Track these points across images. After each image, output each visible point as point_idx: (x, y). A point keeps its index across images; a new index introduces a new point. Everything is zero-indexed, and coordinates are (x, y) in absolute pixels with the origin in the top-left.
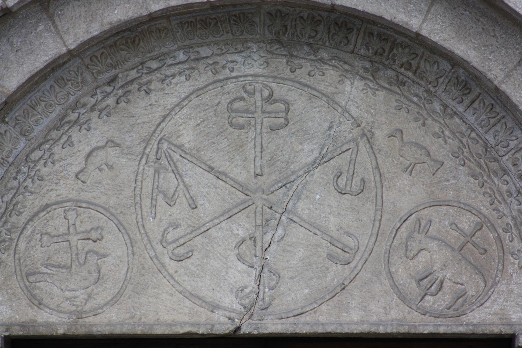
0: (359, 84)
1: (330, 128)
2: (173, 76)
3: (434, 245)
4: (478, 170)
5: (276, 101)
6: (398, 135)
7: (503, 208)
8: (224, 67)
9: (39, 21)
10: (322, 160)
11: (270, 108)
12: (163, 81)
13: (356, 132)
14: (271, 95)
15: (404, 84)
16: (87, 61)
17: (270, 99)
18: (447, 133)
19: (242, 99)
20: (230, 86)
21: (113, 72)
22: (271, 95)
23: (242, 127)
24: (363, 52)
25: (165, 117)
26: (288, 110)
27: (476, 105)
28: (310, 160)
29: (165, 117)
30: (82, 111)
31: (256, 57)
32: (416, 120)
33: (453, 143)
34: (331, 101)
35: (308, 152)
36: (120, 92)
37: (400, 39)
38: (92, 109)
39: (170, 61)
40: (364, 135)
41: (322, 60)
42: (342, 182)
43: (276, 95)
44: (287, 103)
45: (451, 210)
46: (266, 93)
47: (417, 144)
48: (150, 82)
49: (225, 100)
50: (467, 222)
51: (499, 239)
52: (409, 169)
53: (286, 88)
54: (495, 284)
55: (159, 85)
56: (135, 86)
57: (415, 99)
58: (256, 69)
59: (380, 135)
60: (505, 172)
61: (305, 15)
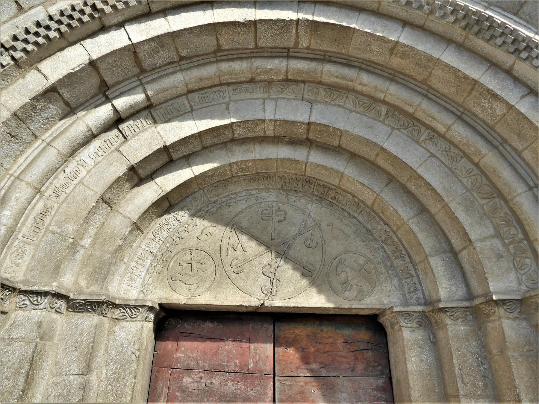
0: (314, 205)
1: (303, 222)
2: (240, 200)
3: (348, 270)
4: (365, 239)
5: (281, 211)
6: (331, 225)
7: (376, 254)
8: (260, 198)
9: (184, 164)
10: (300, 234)
11: (279, 213)
12: (236, 202)
13: (314, 223)
14: (279, 208)
15: (333, 206)
16: (206, 191)
17: (279, 210)
18: (351, 225)
19: (267, 210)
20: (263, 205)
21: (216, 198)
22: (279, 208)
23: (267, 220)
24: (316, 193)
25: (236, 216)
26: (285, 214)
27: (363, 213)
28: (295, 234)
29: (236, 216)
30: (202, 212)
31: (273, 194)
32: (338, 219)
33: (354, 228)
34: (303, 211)
35: (294, 230)
36: (218, 206)
37: (332, 187)
38: (207, 212)
39: (239, 195)
40: (317, 224)
41: (299, 196)
42: (308, 243)
43: (281, 209)
44: (285, 211)
45: (354, 255)
46: (277, 208)
47: (338, 229)
48: (231, 202)
49: (260, 210)
50: (361, 260)
51: (375, 268)
52: (336, 238)
53: (285, 206)
54: (375, 286)
55: (234, 204)
56: (225, 204)
57: (337, 212)
58: (273, 199)
59: (323, 225)
60: (376, 240)
61: (293, 177)
